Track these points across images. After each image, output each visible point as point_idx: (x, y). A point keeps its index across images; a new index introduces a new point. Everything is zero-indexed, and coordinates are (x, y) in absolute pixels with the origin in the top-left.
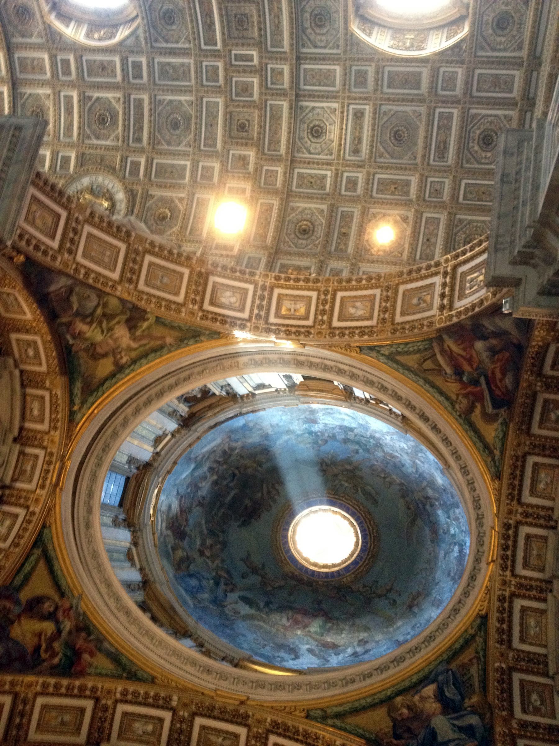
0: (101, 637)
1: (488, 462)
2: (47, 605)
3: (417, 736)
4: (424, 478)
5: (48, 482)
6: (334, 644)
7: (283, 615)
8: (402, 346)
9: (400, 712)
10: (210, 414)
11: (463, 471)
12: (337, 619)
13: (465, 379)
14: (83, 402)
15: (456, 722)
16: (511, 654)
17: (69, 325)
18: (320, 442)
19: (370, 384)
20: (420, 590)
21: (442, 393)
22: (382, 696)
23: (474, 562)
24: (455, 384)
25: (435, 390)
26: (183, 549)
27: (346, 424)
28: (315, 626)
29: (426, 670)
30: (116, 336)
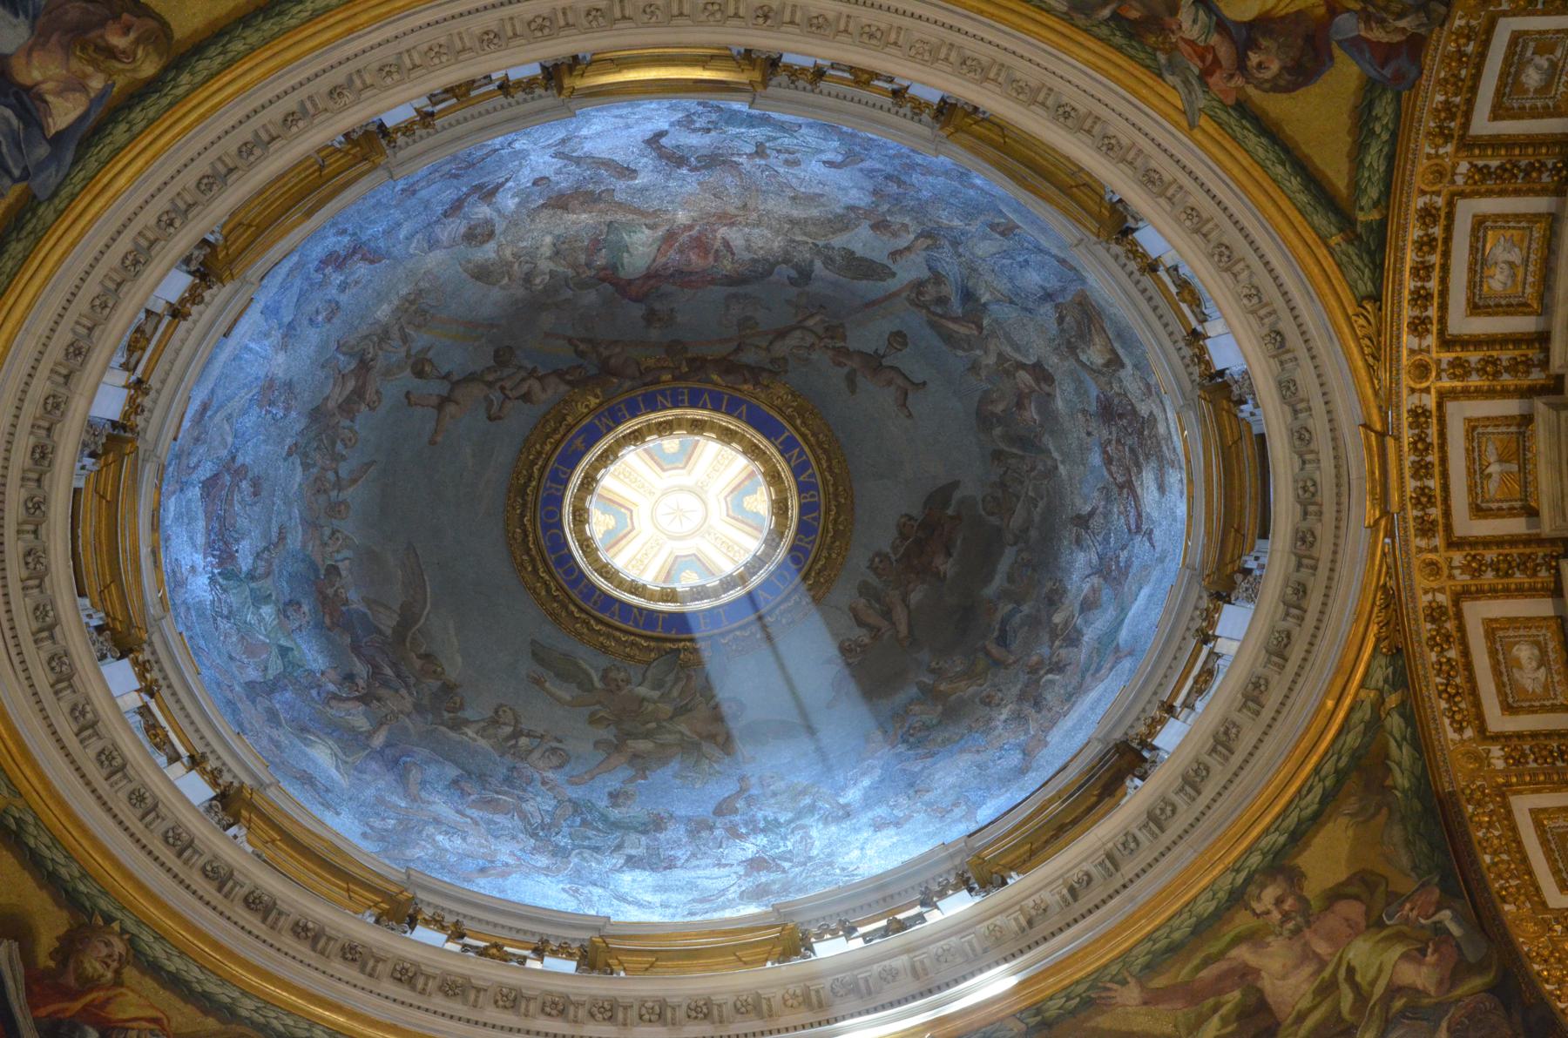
0: (1080, 20)
2: (1275, 67)
5: (1407, 435)
7: (747, 256)
9: (132, 36)
10: (1055, 807)
11: (118, 762)
12: (583, 285)
14: (1375, 724)
17: (1458, 972)
18: (740, 804)
20: (347, 423)
21: (175, 983)
23: (45, 500)
24: (121, 1016)
27: (646, 878)
29: (92, 164)
30: (1307, 970)
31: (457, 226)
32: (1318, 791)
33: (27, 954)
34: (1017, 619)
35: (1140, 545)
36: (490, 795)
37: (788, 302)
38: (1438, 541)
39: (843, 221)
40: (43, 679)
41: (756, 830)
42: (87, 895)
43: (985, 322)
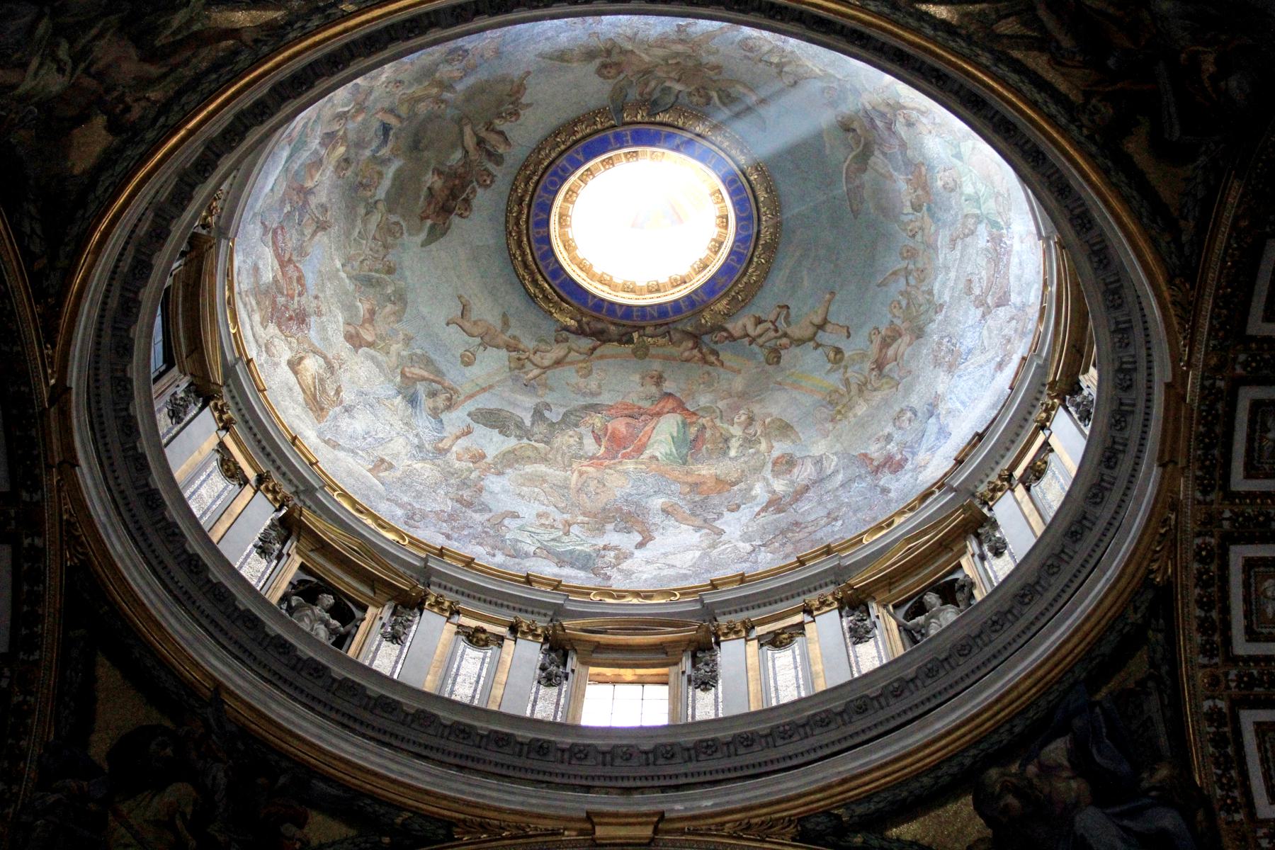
1: (1163, 244)
2: (153, 747)
6: (718, 480)
7: (582, 429)
9: (1002, 804)
15: (1125, 822)
20: (896, 321)
23: (1111, 426)
26: (316, 352)
31: (804, 473)
34: (374, 147)
37: (552, 389)
39: (510, 459)
42: (1106, 158)
43: (398, 379)
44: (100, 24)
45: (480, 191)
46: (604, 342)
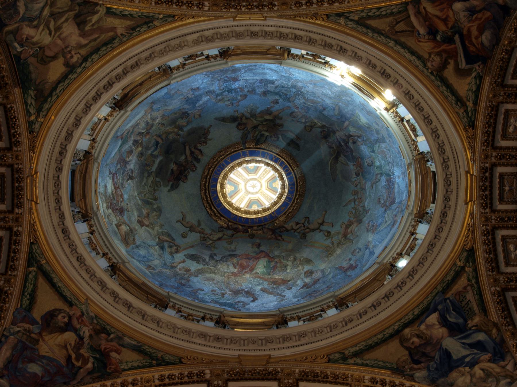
0: (120, 334)
1: (461, 114)
2: (60, 317)
3: (433, 358)
4: (347, 119)
6: (283, 280)
7: (229, 263)
8: (373, 11)
9: (411, 341)
11: (426, 121)
13: (438, 38)
14: (39, 110)
15: (464, 341)
16: (501, 278)
17: (16, 32)
18: (239, 98)
19: (329, 47)
20: (352, 219)
21: (413, 53)
22: (391, 331)
24: (429, 43)
25: (406, 50)
26: (126, 224)
28: (261, 267)
29: (425, 302)
31: (316, 276)
32: (58, 91)
33: (457, 64)
34: (152, 150)
35: (113, 170)
36: (315, 105)
37: (217, 249)
38: (16, 166)
39: (199, 272)
40: (447, 148)
41: (235, 90)
43: (157, 240)
44: (66, 16)
45: (191, 172)
46: (237, 232)
